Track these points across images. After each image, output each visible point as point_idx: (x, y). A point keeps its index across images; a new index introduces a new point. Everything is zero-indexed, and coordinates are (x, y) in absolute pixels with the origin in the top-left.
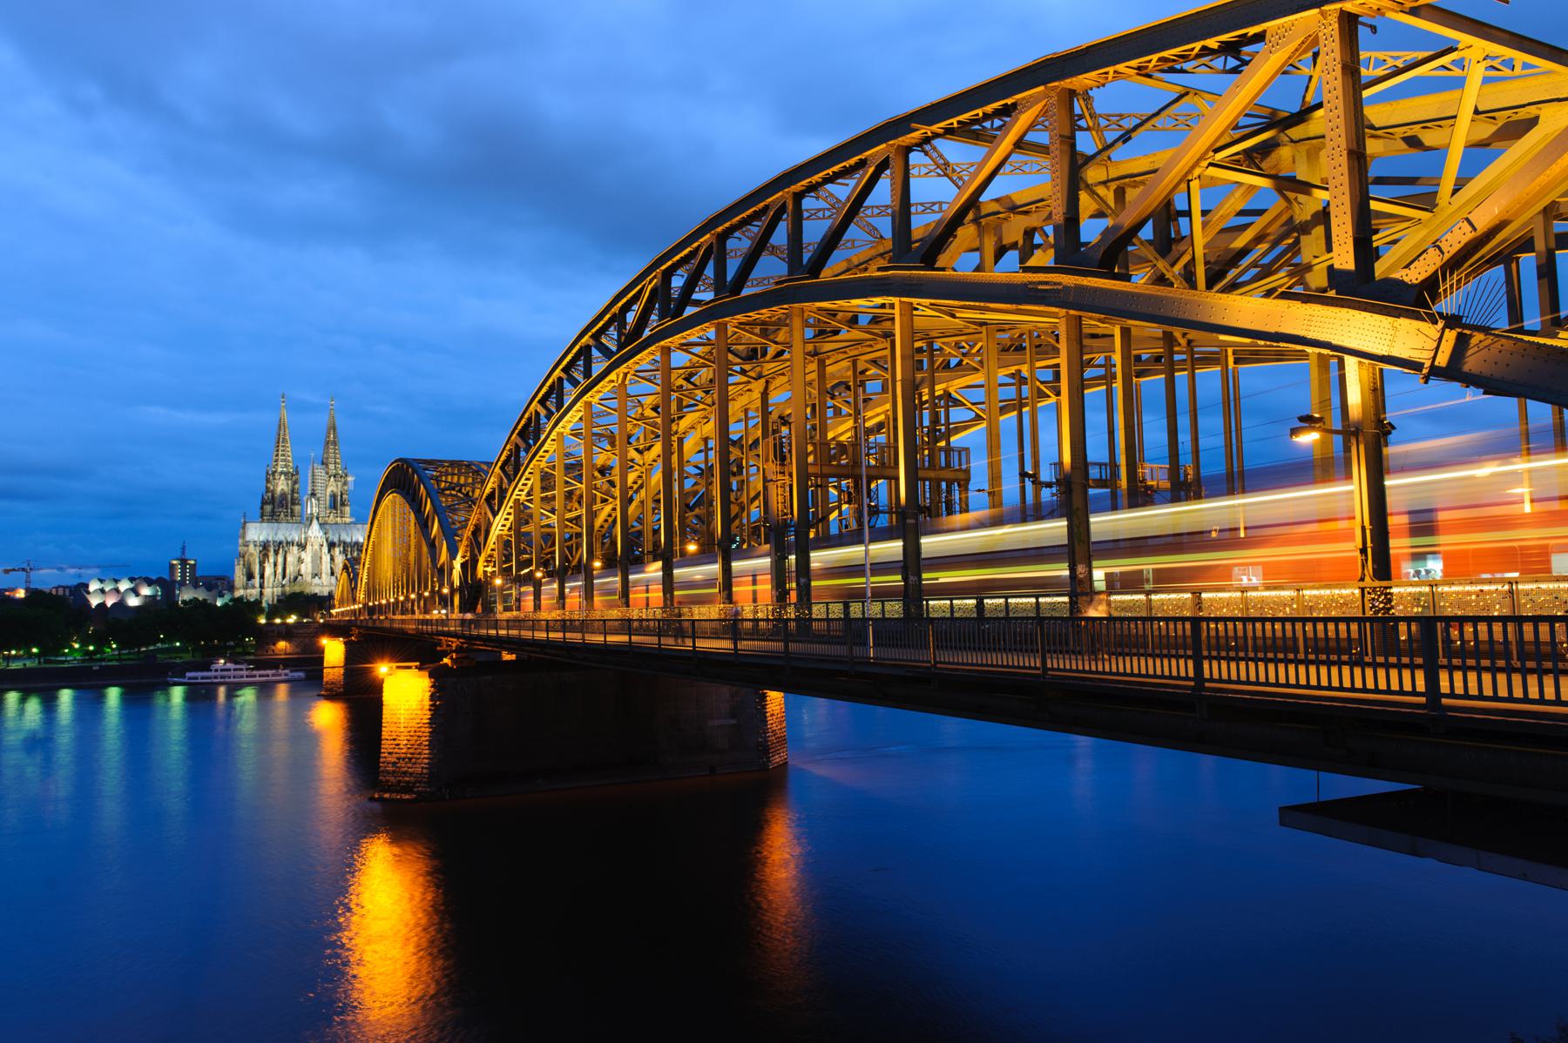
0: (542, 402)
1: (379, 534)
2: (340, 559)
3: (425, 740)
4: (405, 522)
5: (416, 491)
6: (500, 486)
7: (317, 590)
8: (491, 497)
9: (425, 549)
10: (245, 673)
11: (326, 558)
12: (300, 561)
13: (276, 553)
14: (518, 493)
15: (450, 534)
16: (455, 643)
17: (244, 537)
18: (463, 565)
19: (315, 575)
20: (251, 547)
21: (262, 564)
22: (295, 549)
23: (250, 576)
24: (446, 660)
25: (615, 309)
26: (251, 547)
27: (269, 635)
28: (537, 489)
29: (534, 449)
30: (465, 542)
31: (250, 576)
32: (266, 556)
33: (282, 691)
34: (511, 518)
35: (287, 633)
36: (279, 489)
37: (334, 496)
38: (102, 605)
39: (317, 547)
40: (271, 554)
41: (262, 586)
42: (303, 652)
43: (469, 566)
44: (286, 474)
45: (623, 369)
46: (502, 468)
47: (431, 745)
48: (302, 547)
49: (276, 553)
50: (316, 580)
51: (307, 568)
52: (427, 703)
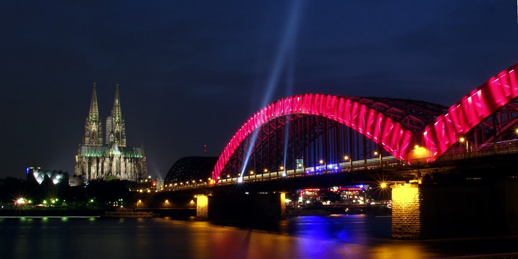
3: (417, 217)
11: (123, 164)
12: (111, 165)
13: (98, 162)
19: (117, 173)
20: (84, 158)
22: (107, 160)
26: (84, 158)
36: (93, 129)
37: (118, 133)
39: (117, 159)
41: (89, 177)
44: (95, 121)
48: (112, 158)
49: (98, 162)
50: (118, 175)
52: (418, 200)
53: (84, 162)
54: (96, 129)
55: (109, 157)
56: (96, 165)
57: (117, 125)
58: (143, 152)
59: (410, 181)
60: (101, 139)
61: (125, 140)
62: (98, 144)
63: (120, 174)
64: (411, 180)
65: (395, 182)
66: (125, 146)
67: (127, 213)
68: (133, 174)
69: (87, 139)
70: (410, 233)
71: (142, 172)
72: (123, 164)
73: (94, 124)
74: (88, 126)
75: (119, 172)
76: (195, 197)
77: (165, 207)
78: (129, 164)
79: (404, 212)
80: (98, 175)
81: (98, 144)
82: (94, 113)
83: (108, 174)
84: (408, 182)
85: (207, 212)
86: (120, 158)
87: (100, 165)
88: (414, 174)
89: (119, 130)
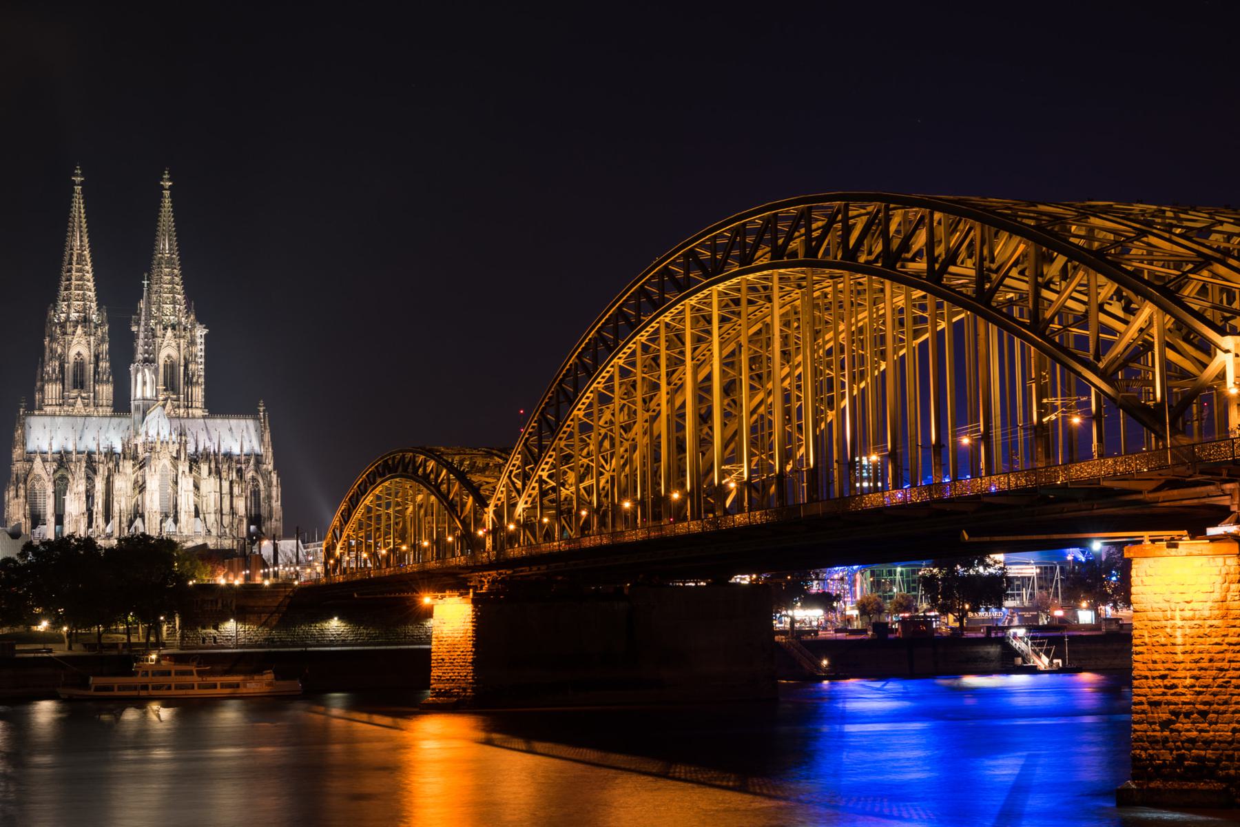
10: (195, 679)
11: (186, 483)
12: (141, 487)
17: (24, 444)
19: (166, 516)
20: (38, 460)
22: (127, 466)
23: (36, 519)
26: (38, 460)
32: (63, 479)
33: (230, 716)
36: (72, 353)
37: (171, 368)
39: (166, 461)
51: (153, 502)
53: (39, 478)
55: (135, 458)
57: (169, 333)
58: (267, 437)
59: (1211, 531)
60: (106, 391)
61: (198, 393)
62: (96, 405)
63: (176, 521)
64: (1215, 525)
65: (1146, 535)
66: (199, 413)
68: (226, 520)
69: (52, 390)
70: (1207, 743)
71: (264, 512)
72: (186, 483)
73: (79, 330)
74: (53, 339)
76: (427, 600)
77: (331, 643)
78: (209, 485)
79: (1180, 657)
80: (90, 525)
81: (96, 405)
82: (80, 292)
83: (131, 523)
84: (1197, 532)
85: (470, 658)
86: (177, 458)
87: (100, 485)
88: (1225, 501)
89: (174, 353)
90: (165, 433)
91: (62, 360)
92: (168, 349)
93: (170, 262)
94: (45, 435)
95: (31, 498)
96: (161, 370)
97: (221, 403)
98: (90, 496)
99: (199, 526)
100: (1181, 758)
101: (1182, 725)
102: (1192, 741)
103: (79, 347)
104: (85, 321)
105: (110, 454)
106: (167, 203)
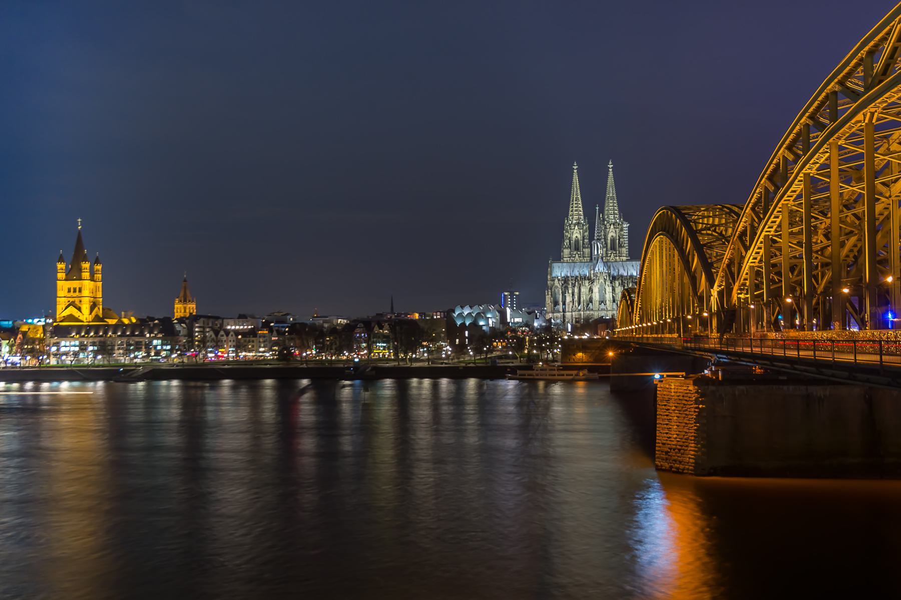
0: (789, 148)
1: (650, 268)
2: (619, 290)
3: (692, 434)
4: (671, 257)
5: (679, 233)
6: (752, 226)
7: (602, 314)
8: (743, 233)
9: (686, 279)
11: (609, 289)
12: (591, 290)
14: (766, 230)
15: (708, 267)
16: (714, 358)
18: (720, 294)
21: (563, 293)
22: (587, 282)
23: (556, 303)
24: (706, 372)
25: (863, 53)
27: (569, 347)
28: (785, 225)
29: (782, 190)
30: (721, 274)
31: (556, 303)
32: (567, 288)
34: (762, 251)
35: (583, 346)
36: (574, 237)
37: (613, 240)
38: (463, 324)
39: (602, 280)
40: (570, 286)
41: (564, 311)
42: (595, 361)
43: (726, 293)
44: (578, 224)
45: (871, 108)
46: (753, 209)
47: (697, 440)
48: (592, 281)
50: (602, 306)
51: (596, 296)
53: (557, 287)
54: (579, 236)
55: (589, 279)
56: (570, 291)
60: (587, 251)
61: (625, 250)
67: (548, 372)
69: (566, 252)
70: (680, 462)
75: (602, 302)
82: (576, 211)
89: (614, 235)
90: (601, 269)
91: (570, 239)
92: (612, 233)
93: (612, 198)
94: (559, 271)
95: (554, 296)
96: (609, 241)
97: (635, 254)
98: (573, 295)
99: (615, 306)
100: (671, 467)
101: (672, 453)
102: (675, 461)
103: (576, 234)
104: (578, 224)
105: (585, 278)
106: (611, 174)
